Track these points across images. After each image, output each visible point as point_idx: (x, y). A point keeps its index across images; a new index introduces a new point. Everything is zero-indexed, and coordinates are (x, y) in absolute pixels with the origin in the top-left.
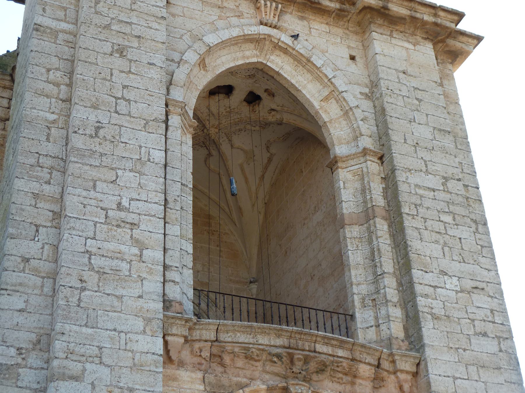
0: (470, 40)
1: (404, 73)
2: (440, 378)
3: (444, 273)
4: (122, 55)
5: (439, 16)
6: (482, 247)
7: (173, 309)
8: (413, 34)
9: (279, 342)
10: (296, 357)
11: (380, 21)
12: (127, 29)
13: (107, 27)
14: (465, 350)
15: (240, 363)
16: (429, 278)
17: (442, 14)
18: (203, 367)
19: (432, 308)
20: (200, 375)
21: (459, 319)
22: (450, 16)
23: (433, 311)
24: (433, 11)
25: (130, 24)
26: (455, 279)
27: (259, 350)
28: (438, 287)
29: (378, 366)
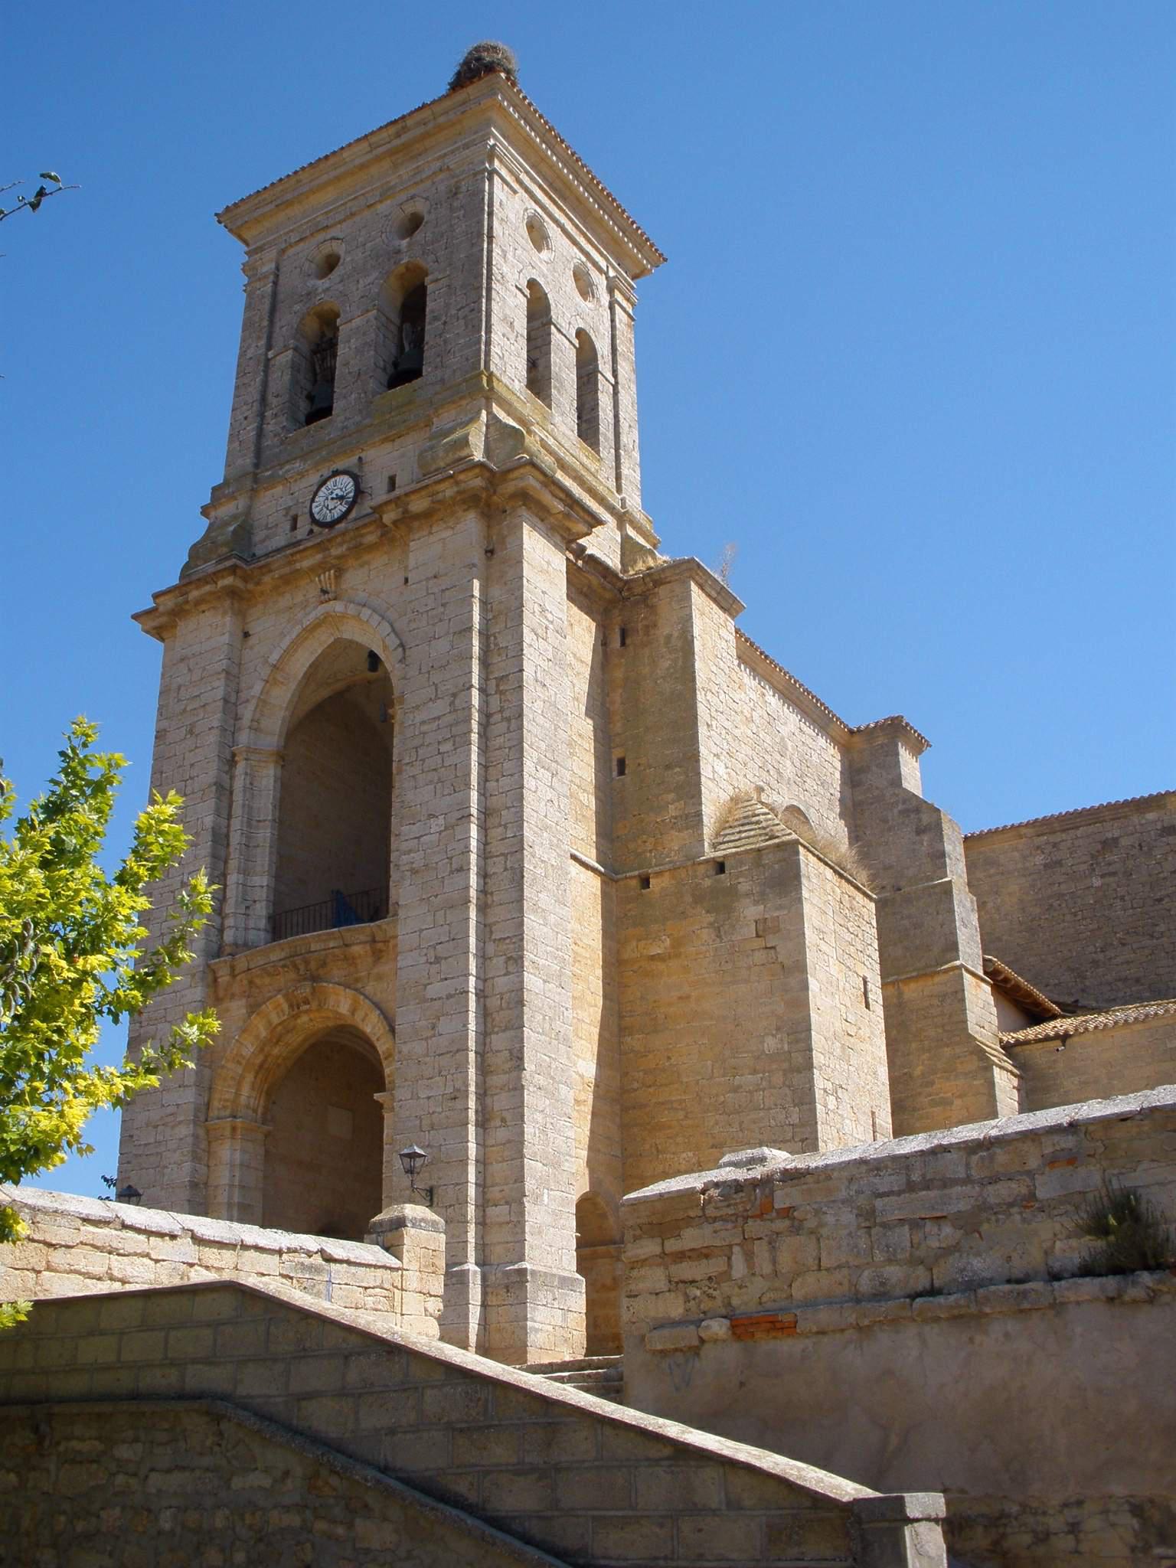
0: (522, 471)
1: (435, 577)
2: (407, 936)
3: (431, 816)
4: (191, 732)
5: (462, 482)
6: (510, 748)
7: (226, 953)
8: (453, 513)
9: (283, 955)
10: (297, 962)
11: (416, 524)
12: (196, 704)
13: (185, 710)
14: (436, 896)
15: (267, 980)
16: (415, 830)
17: (462, 477)
18: (247, 994)
19: (413, 863)
20: (244, 1001)
21: (437, 863)
22: (470, 474)
23: (414, 866)
24: (452, 481)
25: (198, 696)
26: (441, 820)
27: (273, 967)
28: (422, 836)
29: (374, 941)
